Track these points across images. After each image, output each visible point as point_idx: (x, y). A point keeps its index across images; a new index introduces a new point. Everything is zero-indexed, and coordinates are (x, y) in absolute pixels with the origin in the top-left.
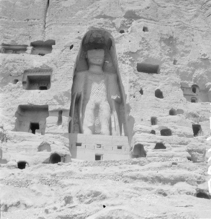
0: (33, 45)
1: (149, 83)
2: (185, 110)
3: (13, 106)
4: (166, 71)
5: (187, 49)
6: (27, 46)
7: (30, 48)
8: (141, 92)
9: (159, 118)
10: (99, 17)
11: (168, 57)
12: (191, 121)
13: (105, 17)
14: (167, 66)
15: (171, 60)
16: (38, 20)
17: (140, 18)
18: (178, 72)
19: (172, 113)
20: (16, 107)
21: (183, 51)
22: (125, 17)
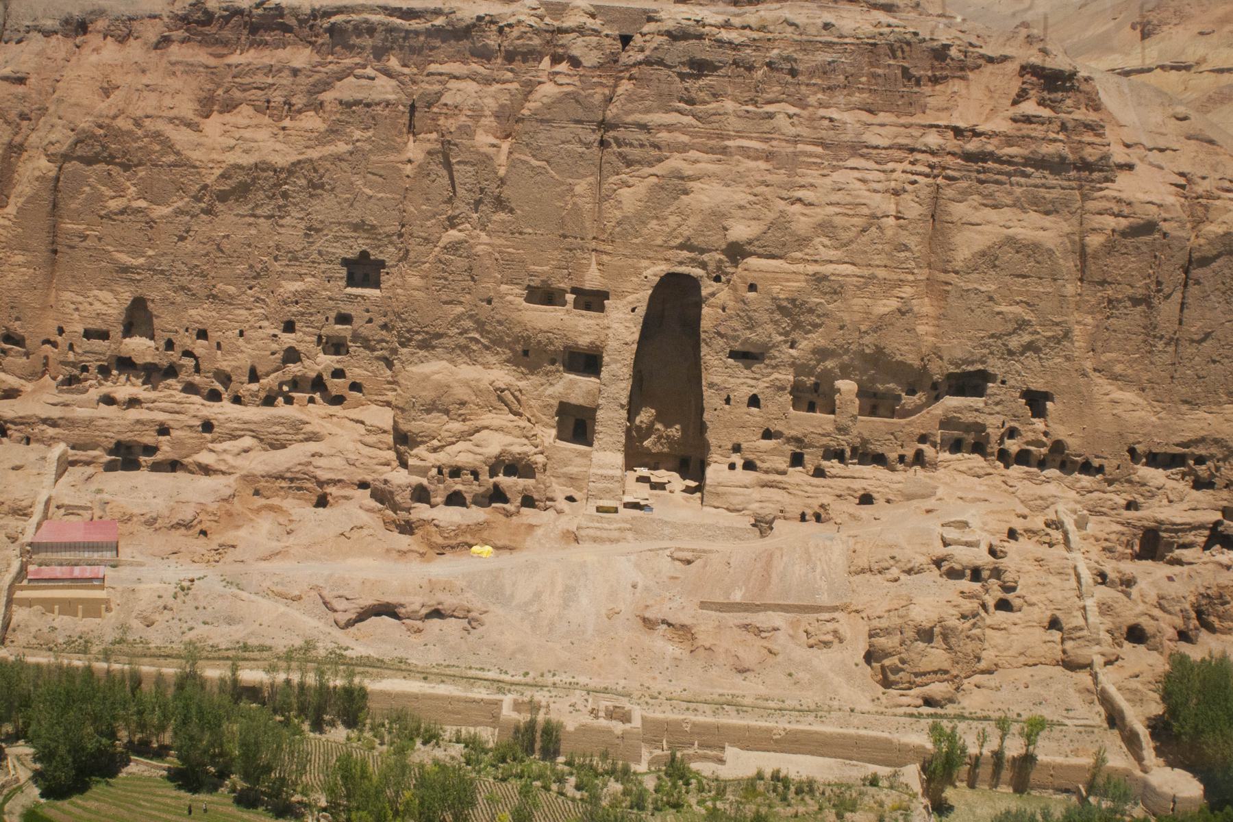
0: (574, 290)
1: (743, 382)
2: (786, 432)
3: (552, 401)
4: (773, 362)
5: (818, 321)
6: (564, 291)
7: (570, 297)
8: (728, 401)
9: (744, 445)
10: (682, 247)
11: (783, 338)
12: (790, 448)
13: (691, 248)
14: (777, 354)
15: (786, 342)
16: (582, 239)
17: (751, 254)
18: (793, 365)
19: (767, 435)
20: (555, 403)
21: (810, 324)
22: (723, 252)
